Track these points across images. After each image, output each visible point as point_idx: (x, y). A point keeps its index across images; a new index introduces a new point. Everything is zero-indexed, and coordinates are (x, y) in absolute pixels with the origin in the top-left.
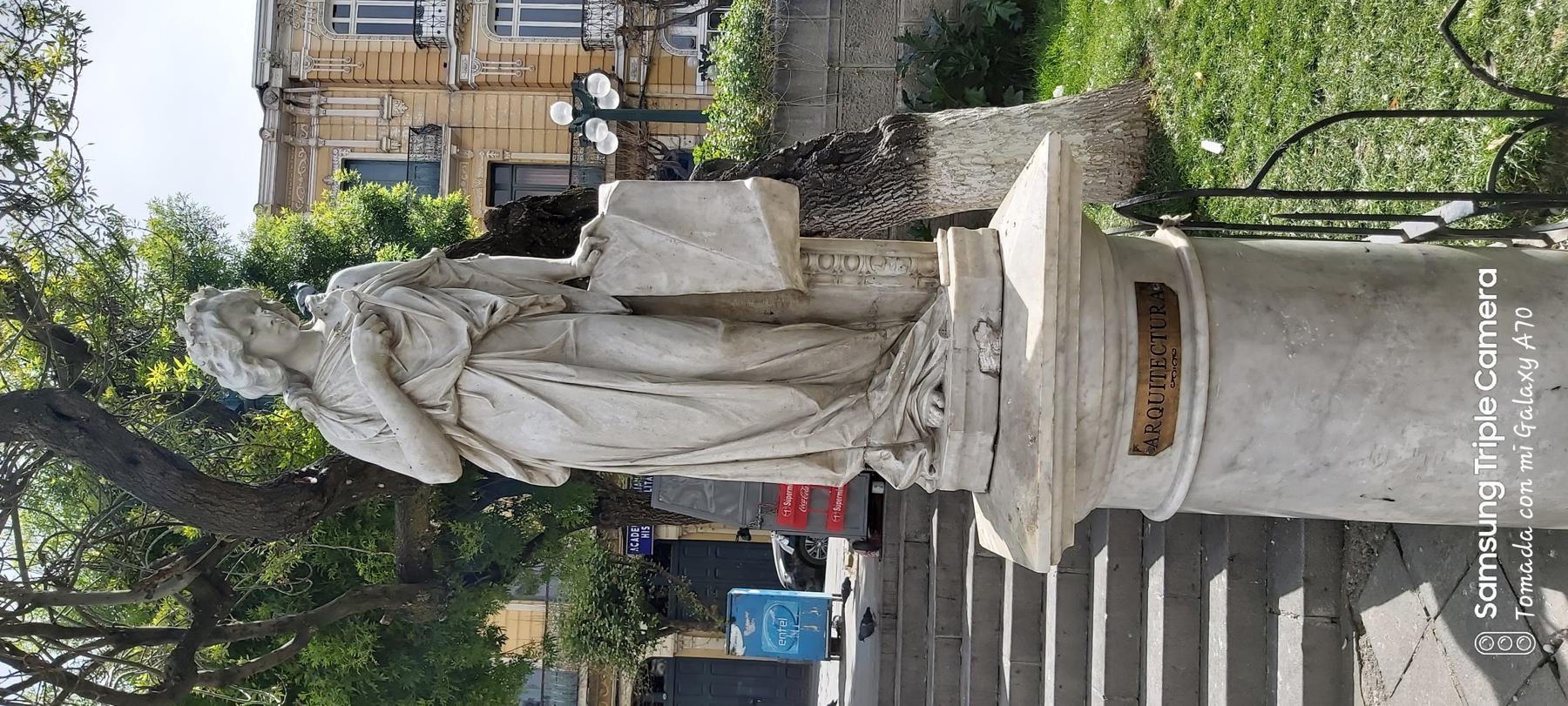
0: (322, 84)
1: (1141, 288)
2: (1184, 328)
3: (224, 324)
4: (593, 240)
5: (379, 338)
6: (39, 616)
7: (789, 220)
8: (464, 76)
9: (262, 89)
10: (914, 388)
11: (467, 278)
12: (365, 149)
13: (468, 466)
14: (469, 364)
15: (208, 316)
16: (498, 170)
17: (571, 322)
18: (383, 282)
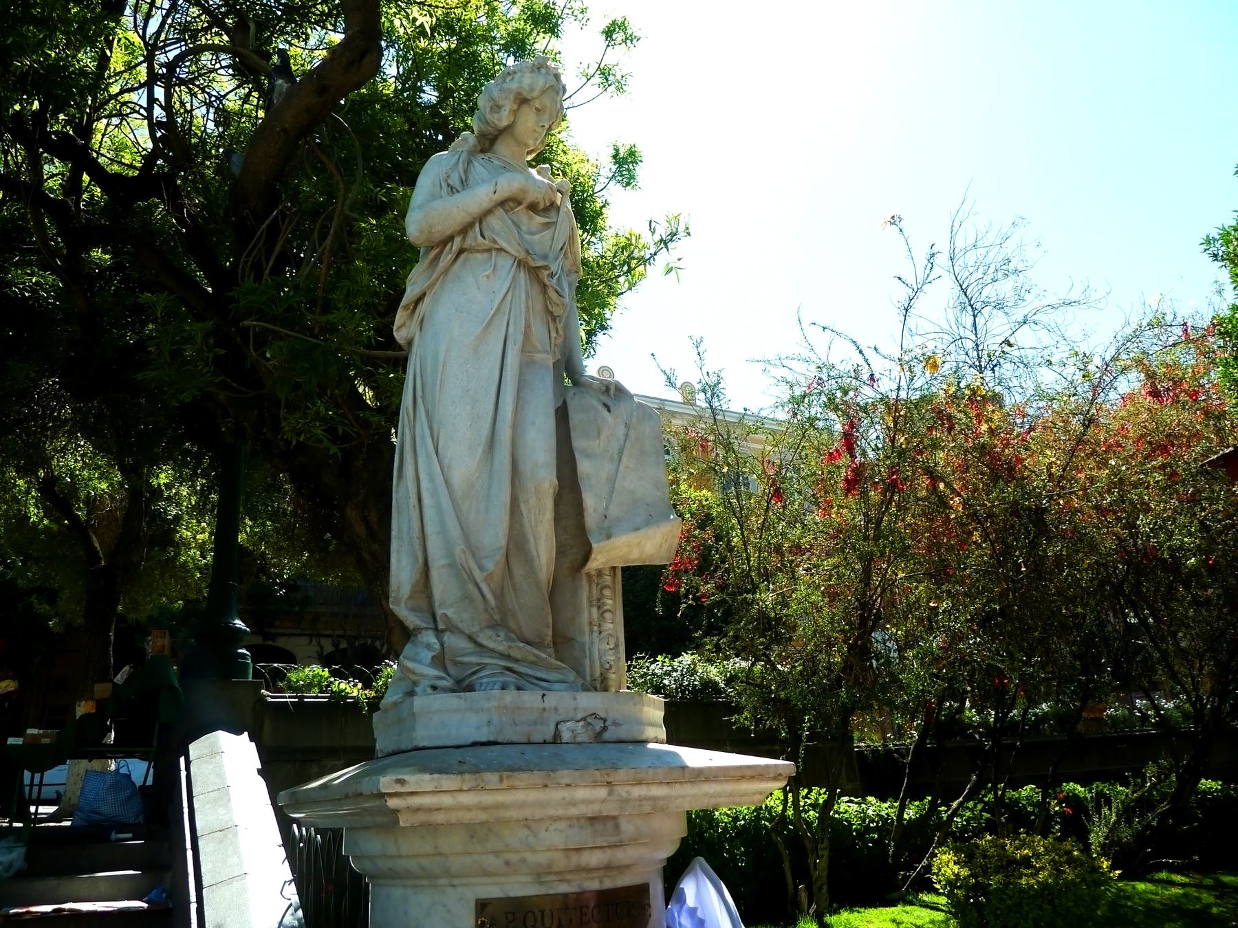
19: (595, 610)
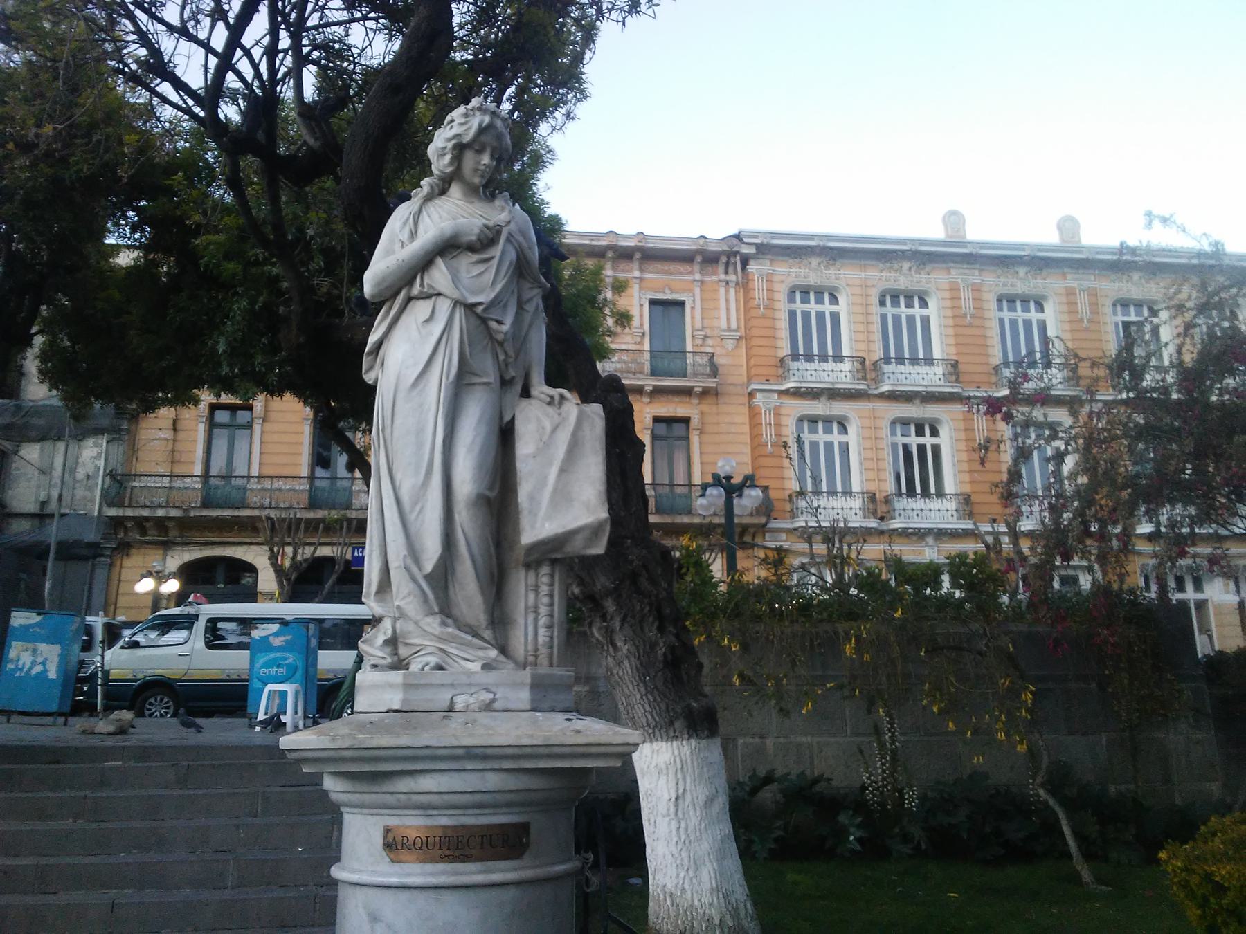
0: (745, 284)
1: (524, 828)
2: (489, 863)
3: (482, 130)
4: (557, 398)
5: (474, 238)
6: (285, 42)
7: (576, 547)
8: (759, 395)
9: (738, 237)
10: (441, 649)
11: (527, 307)
12: (693, 317)
13: (378, 306)
14: (456, 303)
15: (487, 119)
16: (683, 426)
17: (491, 380)
18: (520, 244)
19: (532, 596)
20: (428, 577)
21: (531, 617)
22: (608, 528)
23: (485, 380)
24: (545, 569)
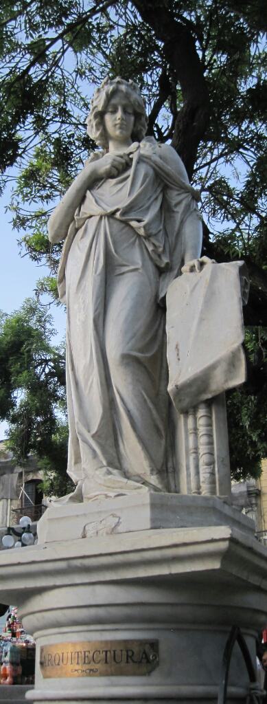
1: (154, 645)
3: (110, 97)
5: (108, 167)
7: (220, 383)
19: (191, 438)
20: (93, 436)
21: (192, 457)
22: (243, 356)
23: (132, 267)
24: (202, 412)
